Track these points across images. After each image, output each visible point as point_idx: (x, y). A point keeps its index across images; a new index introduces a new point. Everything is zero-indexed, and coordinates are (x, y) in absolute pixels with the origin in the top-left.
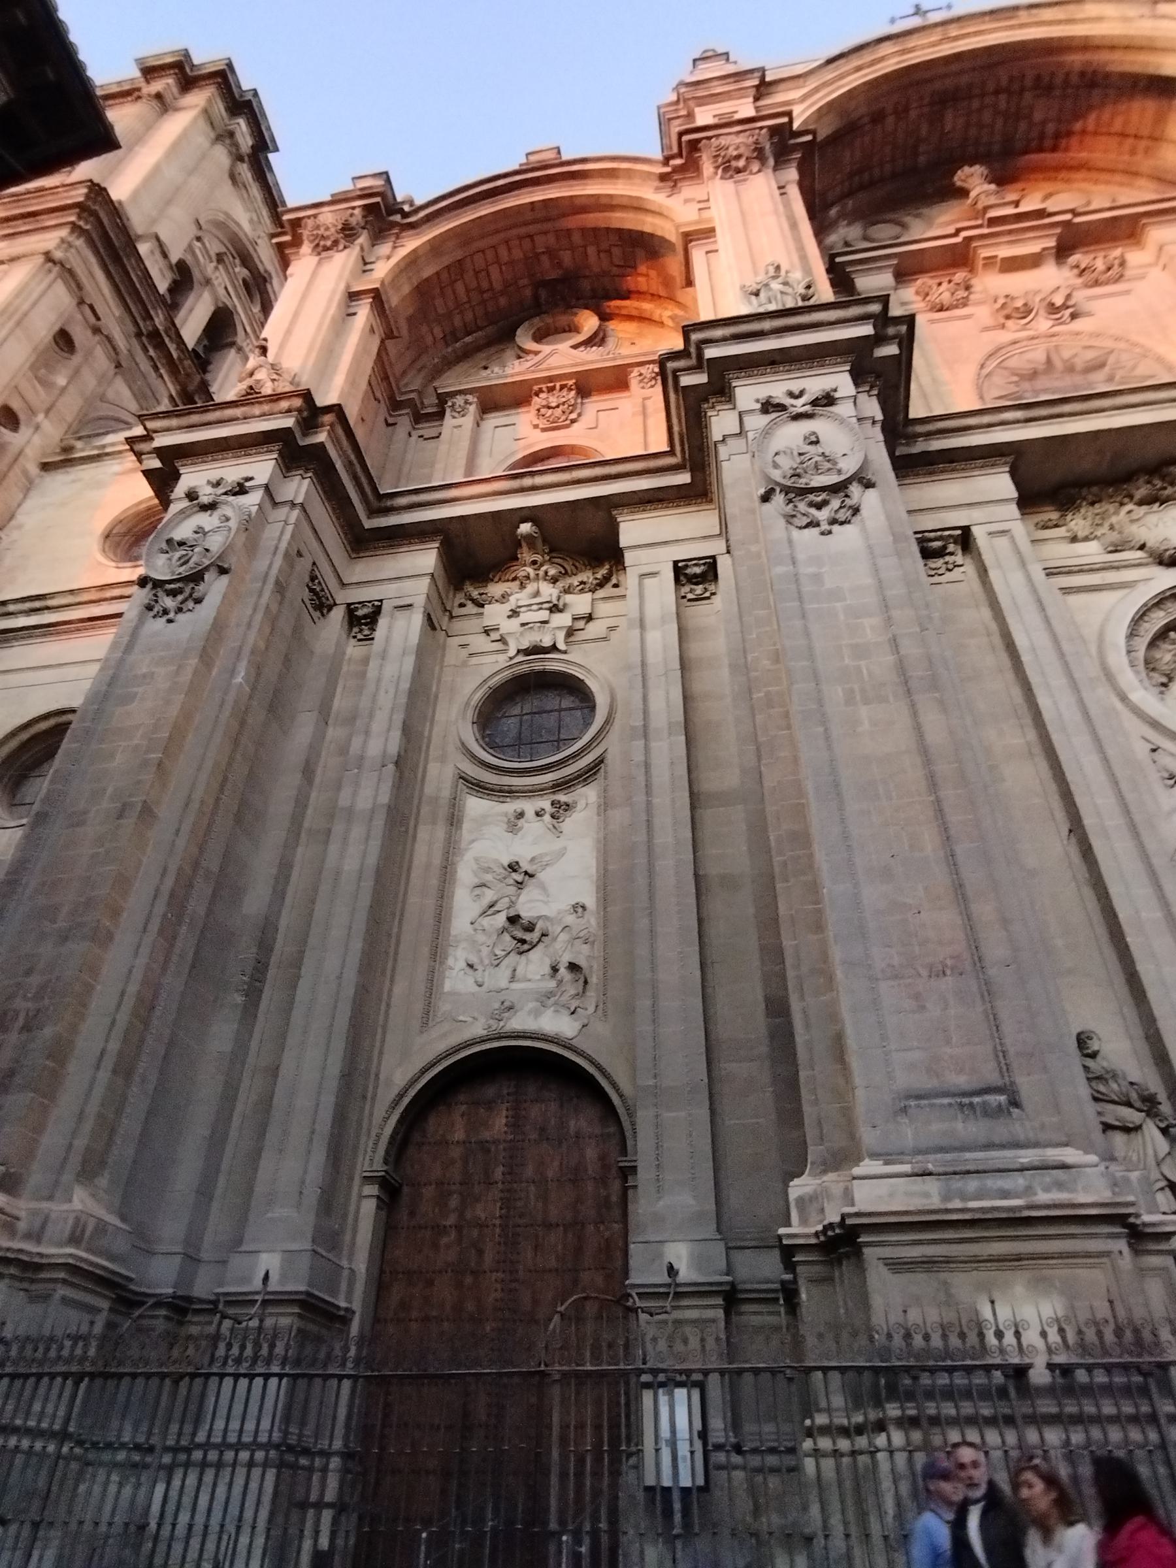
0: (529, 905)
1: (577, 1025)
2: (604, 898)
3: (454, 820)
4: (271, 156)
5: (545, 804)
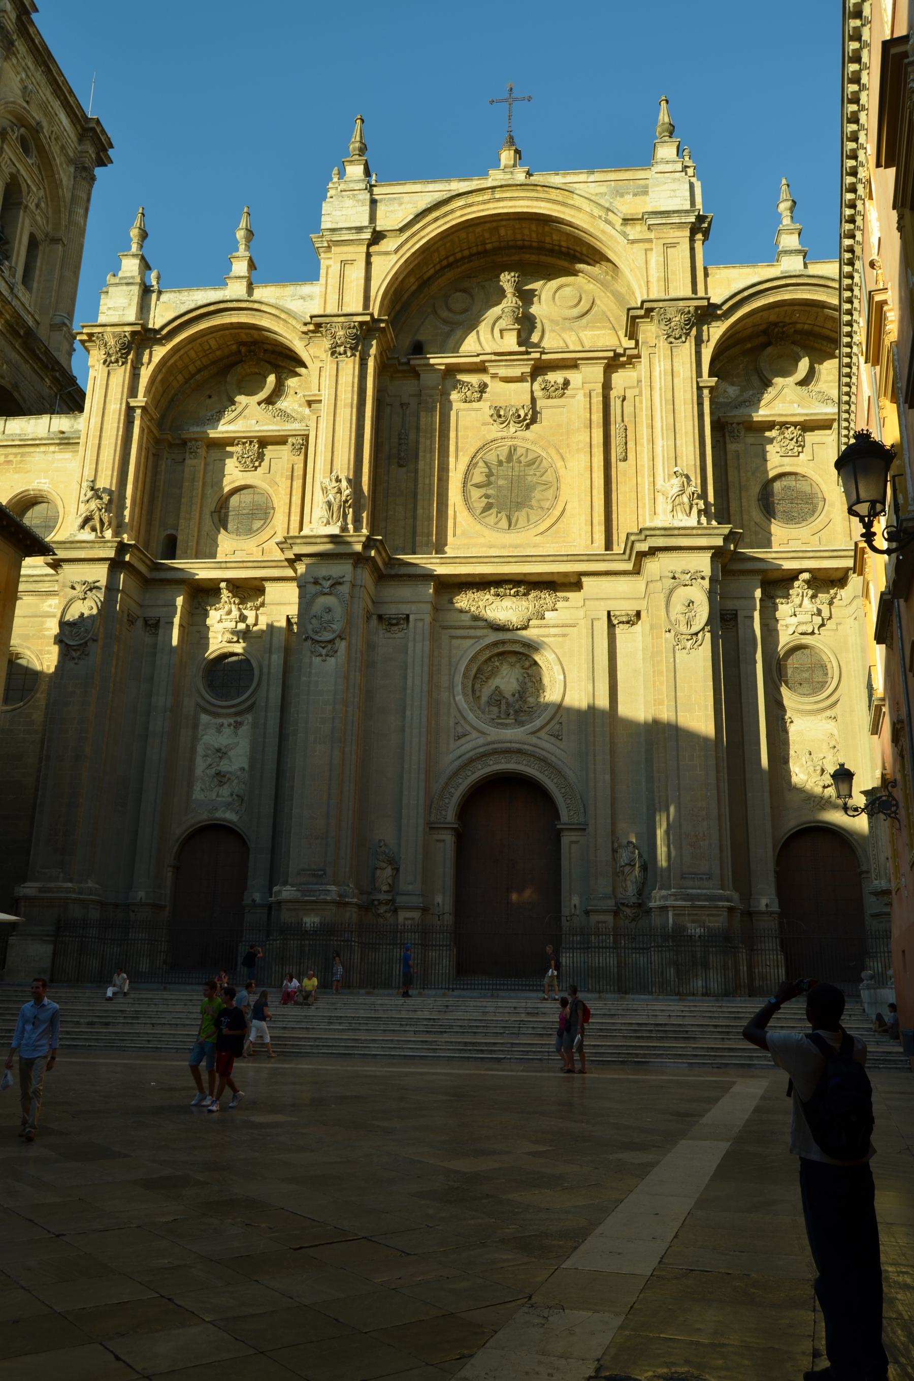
0: (224, 766)
1: (238, 817)
2: (252, 766)
3: (195, 726)
4: (34, 16)
5: (231, 721)
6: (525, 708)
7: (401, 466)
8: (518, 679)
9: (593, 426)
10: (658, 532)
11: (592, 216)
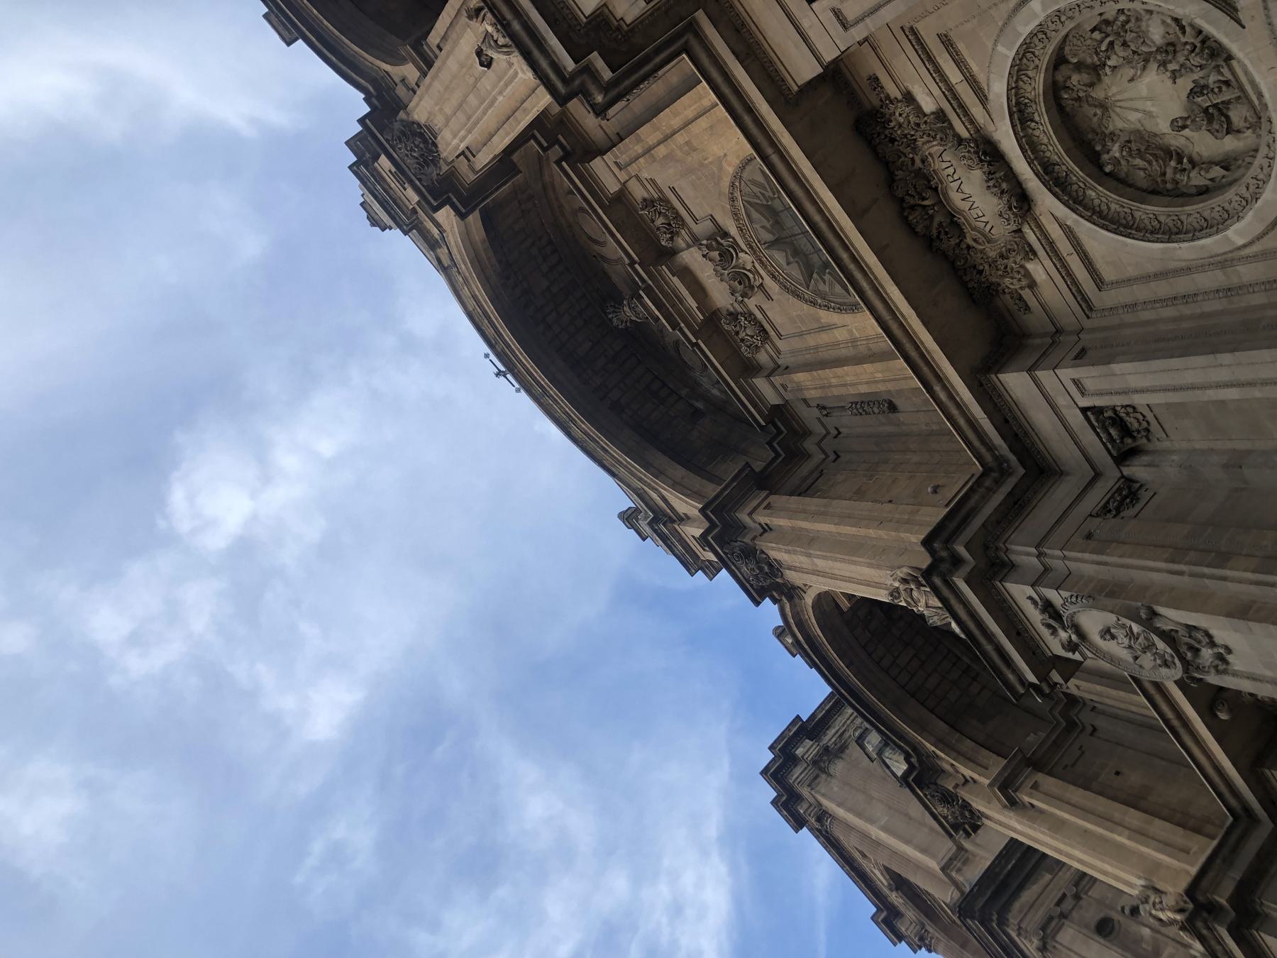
6: (1189, 37)
7: (893, 408)
8: (1131, 80)
9: (646, 146)
10: (544, 64)
11: (466, 281)
